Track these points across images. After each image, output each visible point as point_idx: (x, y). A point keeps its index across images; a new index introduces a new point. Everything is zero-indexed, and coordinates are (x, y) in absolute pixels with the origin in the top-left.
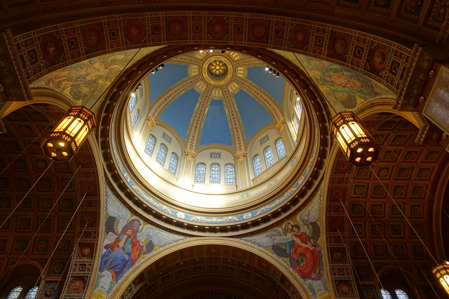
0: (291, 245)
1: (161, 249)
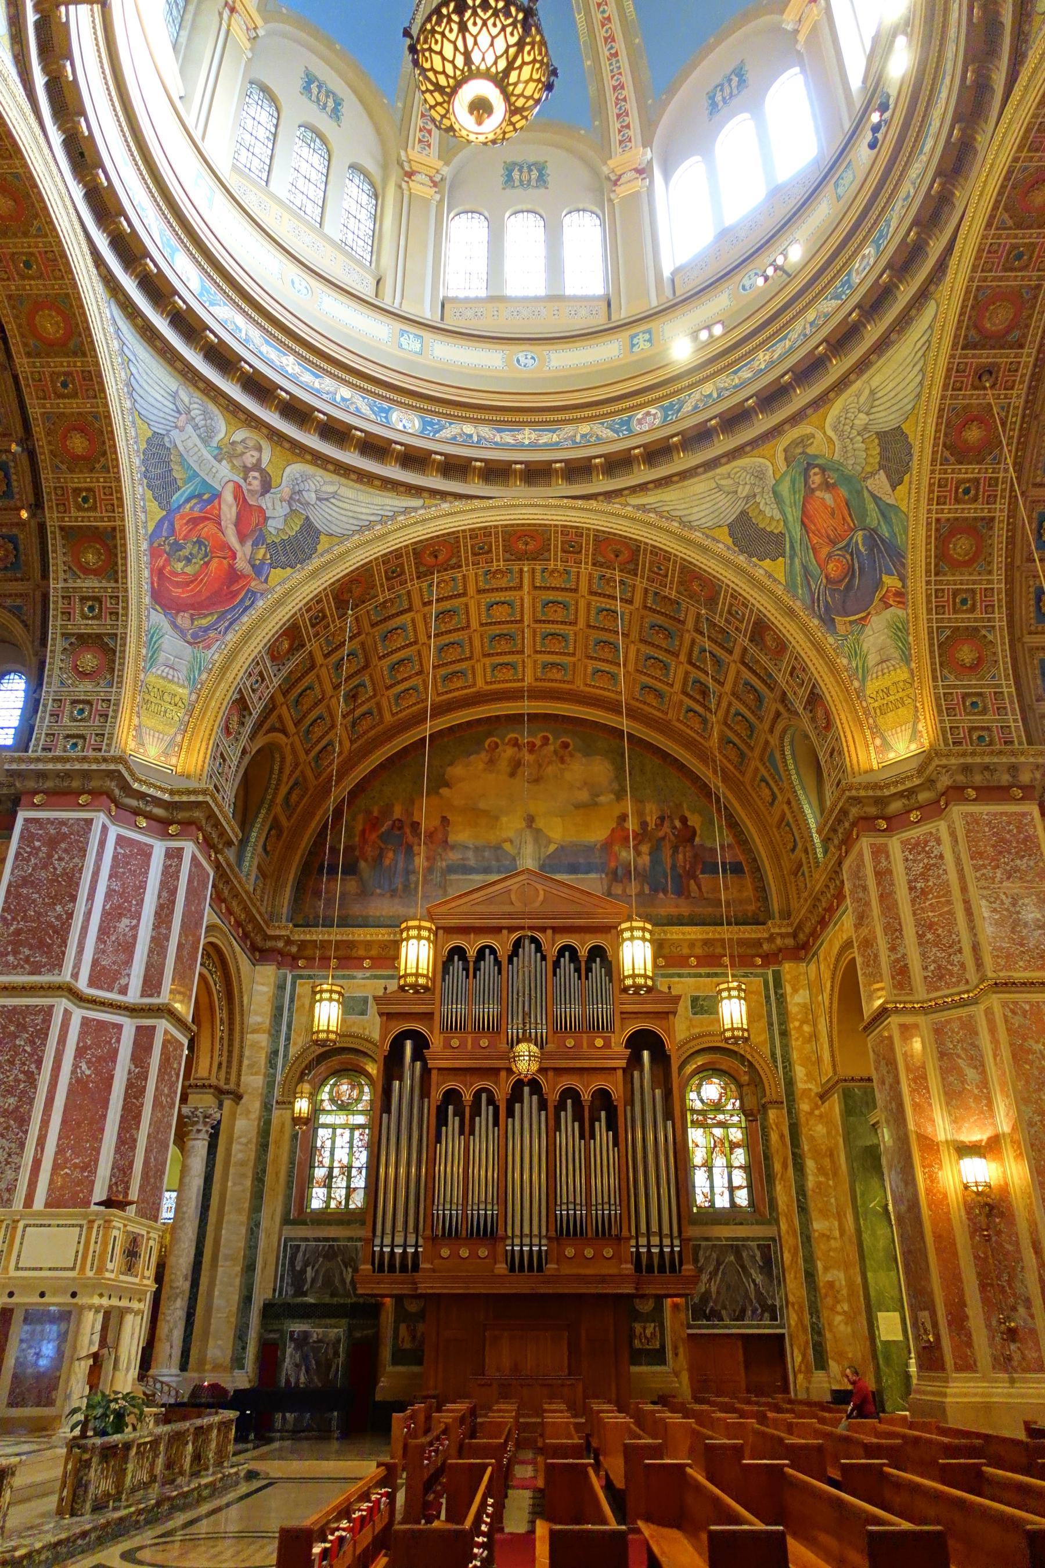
0: (200, 496)
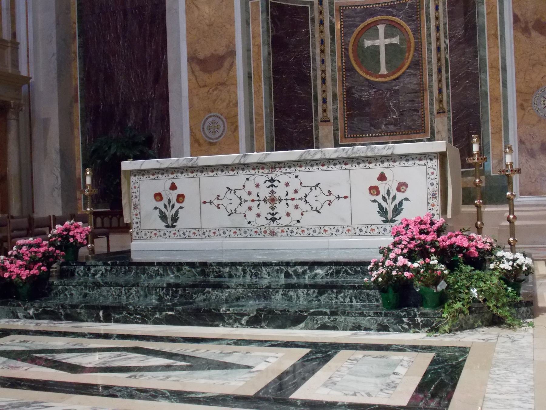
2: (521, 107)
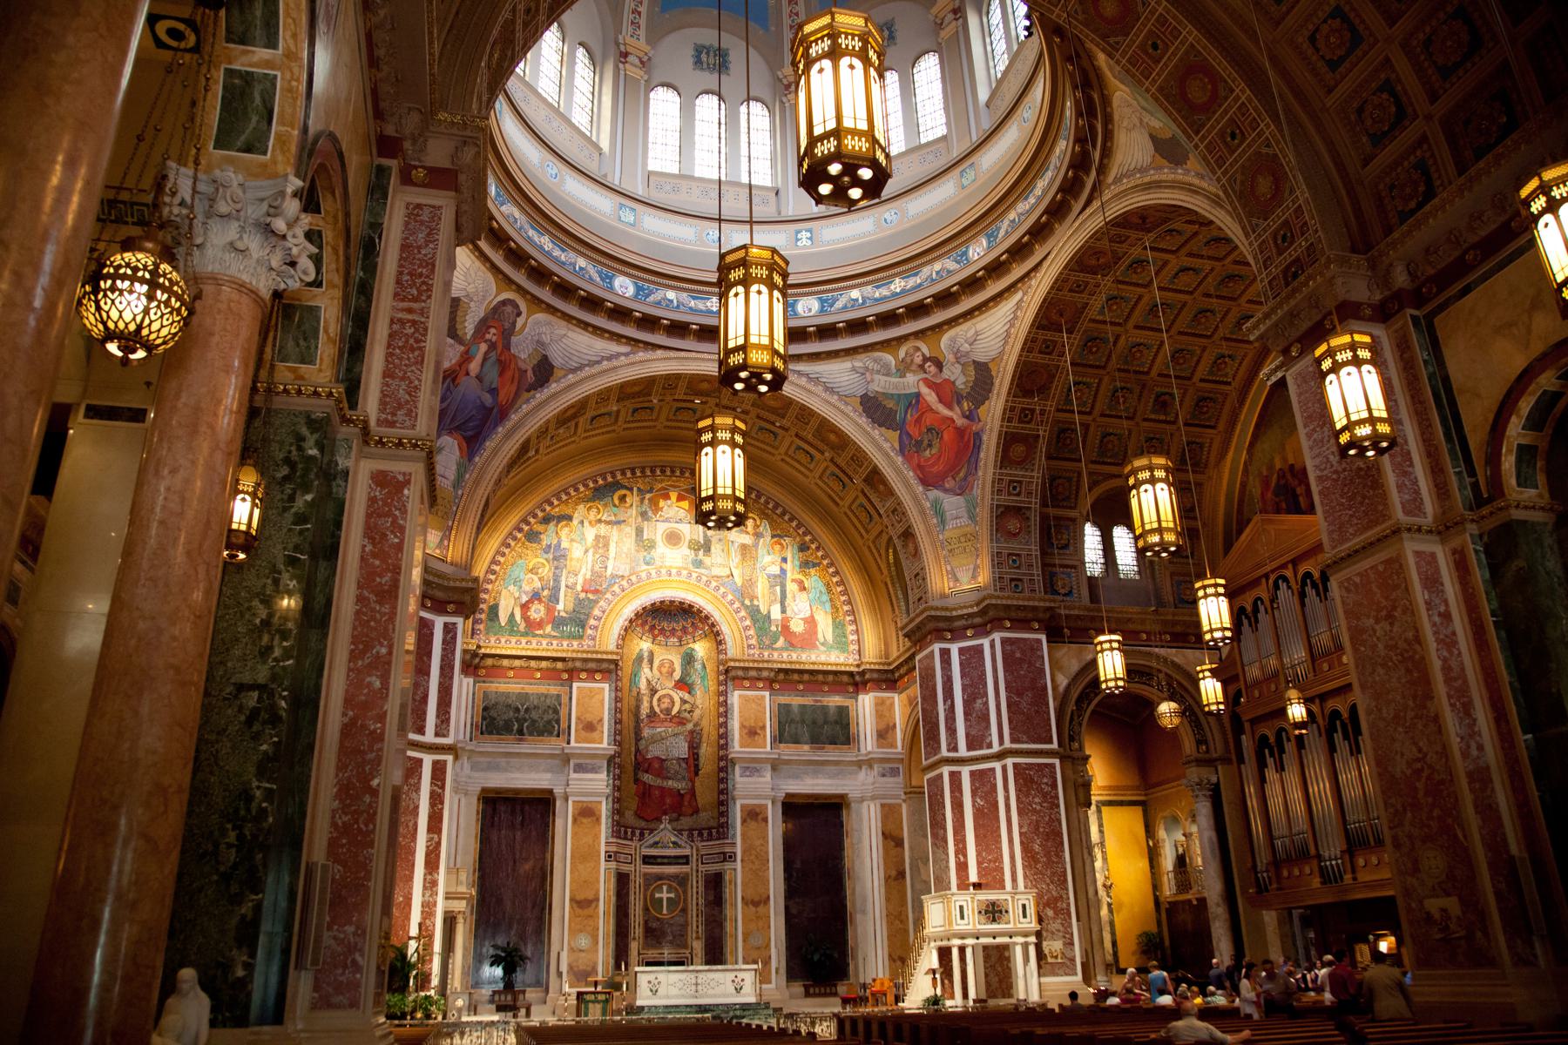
0: (910, 404)
1: (570, 376)
2: (744, 941)
